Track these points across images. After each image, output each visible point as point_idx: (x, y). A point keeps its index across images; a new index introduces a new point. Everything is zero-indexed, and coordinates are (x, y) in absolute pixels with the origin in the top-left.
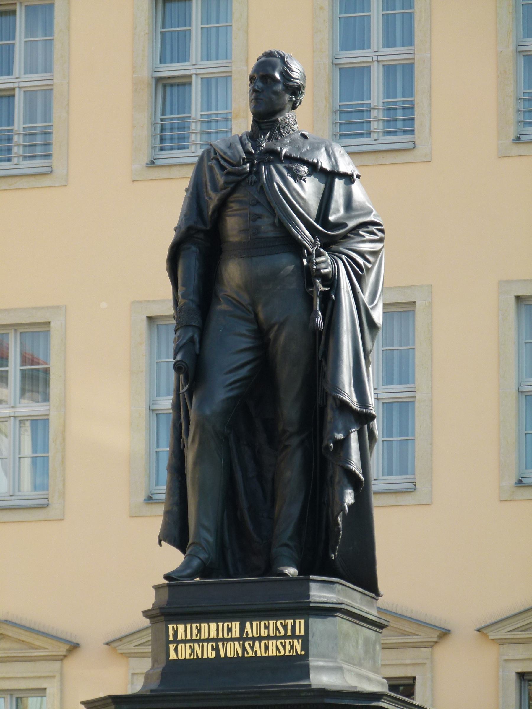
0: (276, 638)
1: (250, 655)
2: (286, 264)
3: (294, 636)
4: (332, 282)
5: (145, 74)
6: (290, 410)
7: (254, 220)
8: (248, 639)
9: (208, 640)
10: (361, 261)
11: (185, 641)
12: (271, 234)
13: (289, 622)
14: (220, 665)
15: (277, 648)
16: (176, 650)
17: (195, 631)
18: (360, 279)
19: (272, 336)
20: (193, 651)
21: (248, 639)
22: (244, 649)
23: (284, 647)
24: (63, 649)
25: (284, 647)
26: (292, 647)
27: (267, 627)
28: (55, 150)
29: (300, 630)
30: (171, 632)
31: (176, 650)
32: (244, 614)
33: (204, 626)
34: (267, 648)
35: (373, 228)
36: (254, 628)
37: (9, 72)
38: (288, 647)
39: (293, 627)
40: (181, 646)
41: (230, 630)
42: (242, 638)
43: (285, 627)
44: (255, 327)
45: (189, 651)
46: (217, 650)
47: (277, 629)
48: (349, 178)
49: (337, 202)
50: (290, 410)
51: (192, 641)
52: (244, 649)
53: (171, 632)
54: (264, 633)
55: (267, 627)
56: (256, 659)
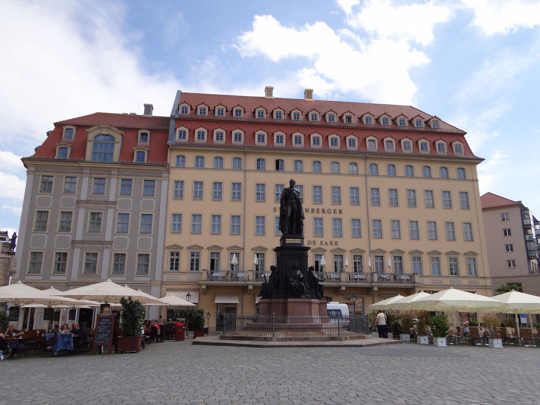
6: (295, 217)
14: (292, 244)
32: (295, 238)
50: (295, 217)
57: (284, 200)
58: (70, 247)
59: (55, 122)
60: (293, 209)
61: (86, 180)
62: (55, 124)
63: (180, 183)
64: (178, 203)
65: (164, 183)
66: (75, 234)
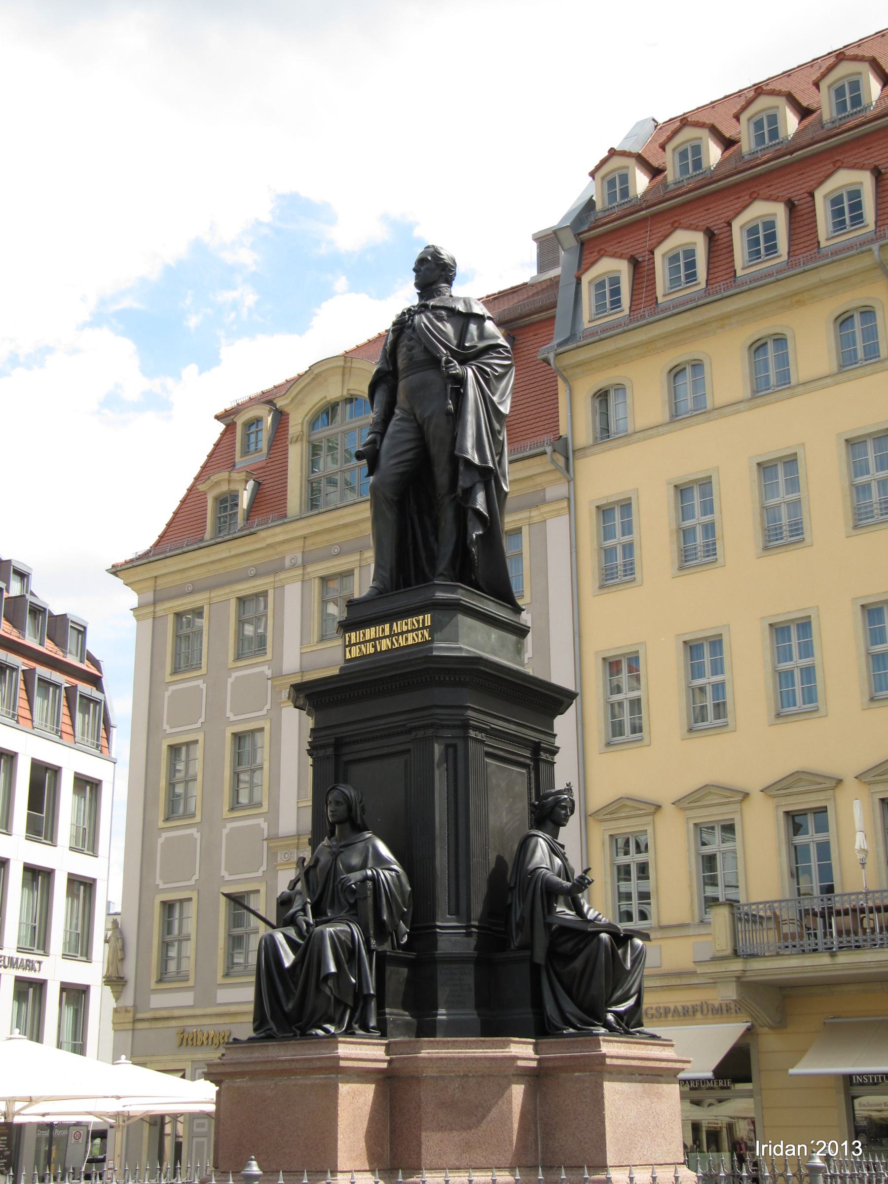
0: (412, 631)
1: (397, 645)
2: (430, 375)
3: (424, 628)
4: (461, 381)
5: (674, 527)
6: (442, 478)
7: (410, 350)
8: (395, 635)
9: (370, 641)
10: (488, 369)
11: (355, 644)
12: (422, 358)
13: (421, 617)
15: (413, 639)
16: (350, 652)
17: (362, 635)
18: (487, 382)
19: (425, 428)
20: (360, 649)
21: (395, 635)
22: (392, 643)
23: (417, 636)
24: (653, 809)
25: (417, 636)
26: (423, 635)
27: (406, 624)
28: (637, 570)
29: (428, 623)
30: (347, 639)
31: (350, 652)
33: (367, 630)
34: (407, 639)
35: (501, 350)
36: (400, 626)
37: (791, 660)
38: (420, 636)
39: (424, 620)
40: (353, 648)
41: (383, 630)
42: (390, 636)
43: (418, 622)
44: (415, 425)
45: (358, 651)
46: (375, 646)
47: (413, 624)
48: (480, 319)
49: (472, 334)
51: (360, 643)
52: (392, 643)
53: (347, 639)
54: (405, 628)
55: (406, 624)
56: (400, 648)
57: (380, 396)
58: (264, 868)
59: (220, 410)
60: (420, 430)
61: (293, 593)
62: (217, 417)
63: (616, 514)
64: (620, 600)
65: (557, 529)
66: (273, 816)
